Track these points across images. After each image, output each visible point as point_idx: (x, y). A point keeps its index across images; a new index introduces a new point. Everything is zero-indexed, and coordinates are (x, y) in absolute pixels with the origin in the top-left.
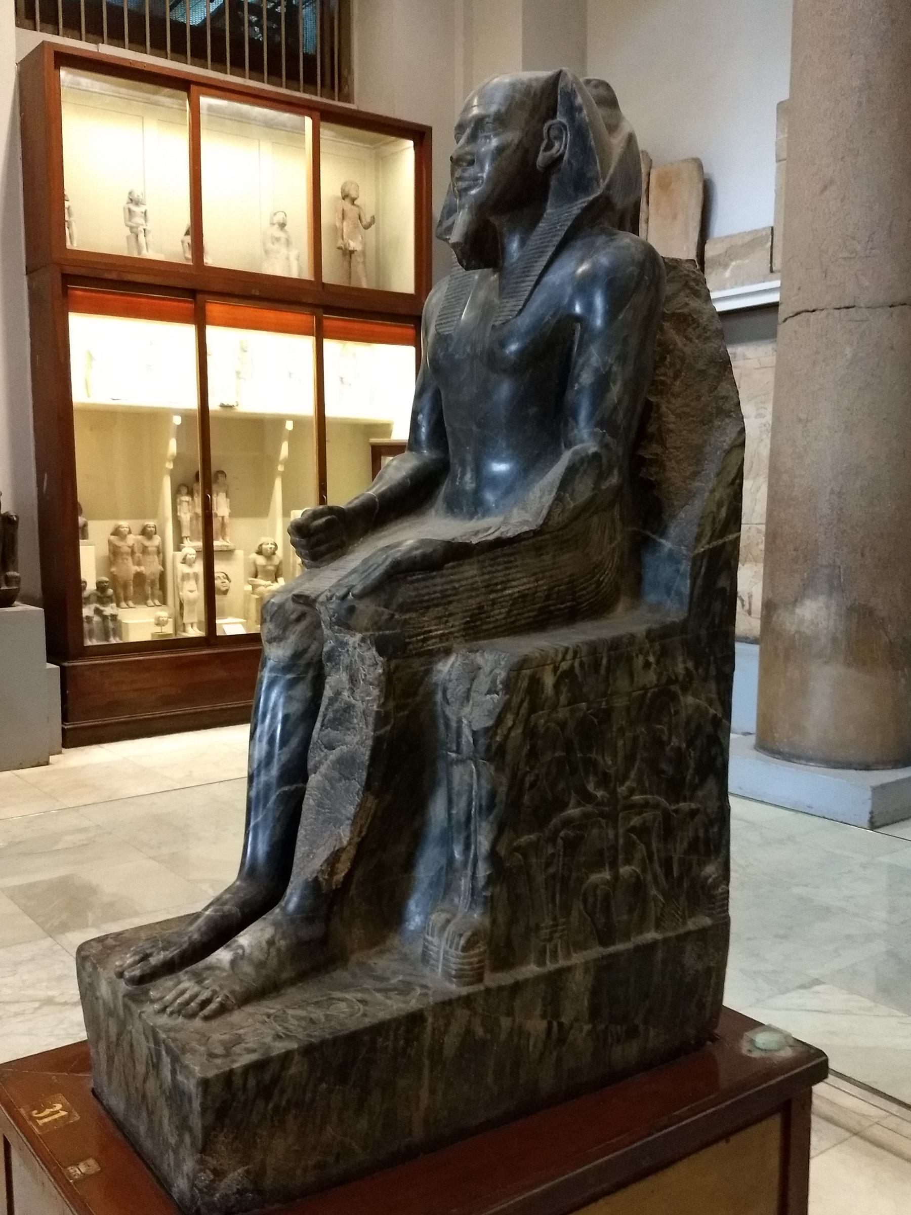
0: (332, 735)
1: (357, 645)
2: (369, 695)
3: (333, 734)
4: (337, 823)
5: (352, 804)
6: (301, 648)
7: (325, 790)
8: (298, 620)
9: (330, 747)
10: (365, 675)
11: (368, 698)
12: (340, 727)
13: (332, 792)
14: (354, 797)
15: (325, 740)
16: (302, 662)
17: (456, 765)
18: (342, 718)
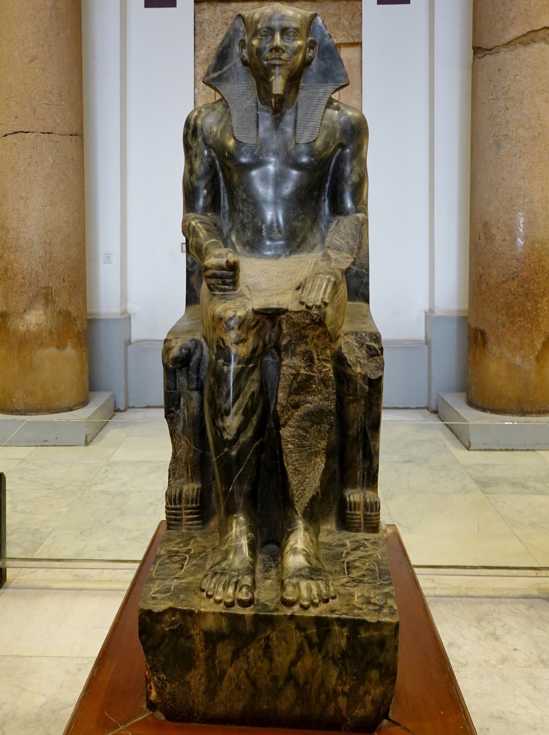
0: (296, 399)
1: (315, 336)
2: (325, 367)
3: (297, 398)
4: (317, 454)
5: (323, 439)
6: (256, 346)
7: (300, 436)
8: (255, 326)
9: (296, 406)
10: (318, 356)
11: (324, 370)
12: (302, 393)
13: (308, 435)
14: (325, 434)
15: (292, 403)
16: (257, 354)
17: (353, 403)
18: (302, 386)
